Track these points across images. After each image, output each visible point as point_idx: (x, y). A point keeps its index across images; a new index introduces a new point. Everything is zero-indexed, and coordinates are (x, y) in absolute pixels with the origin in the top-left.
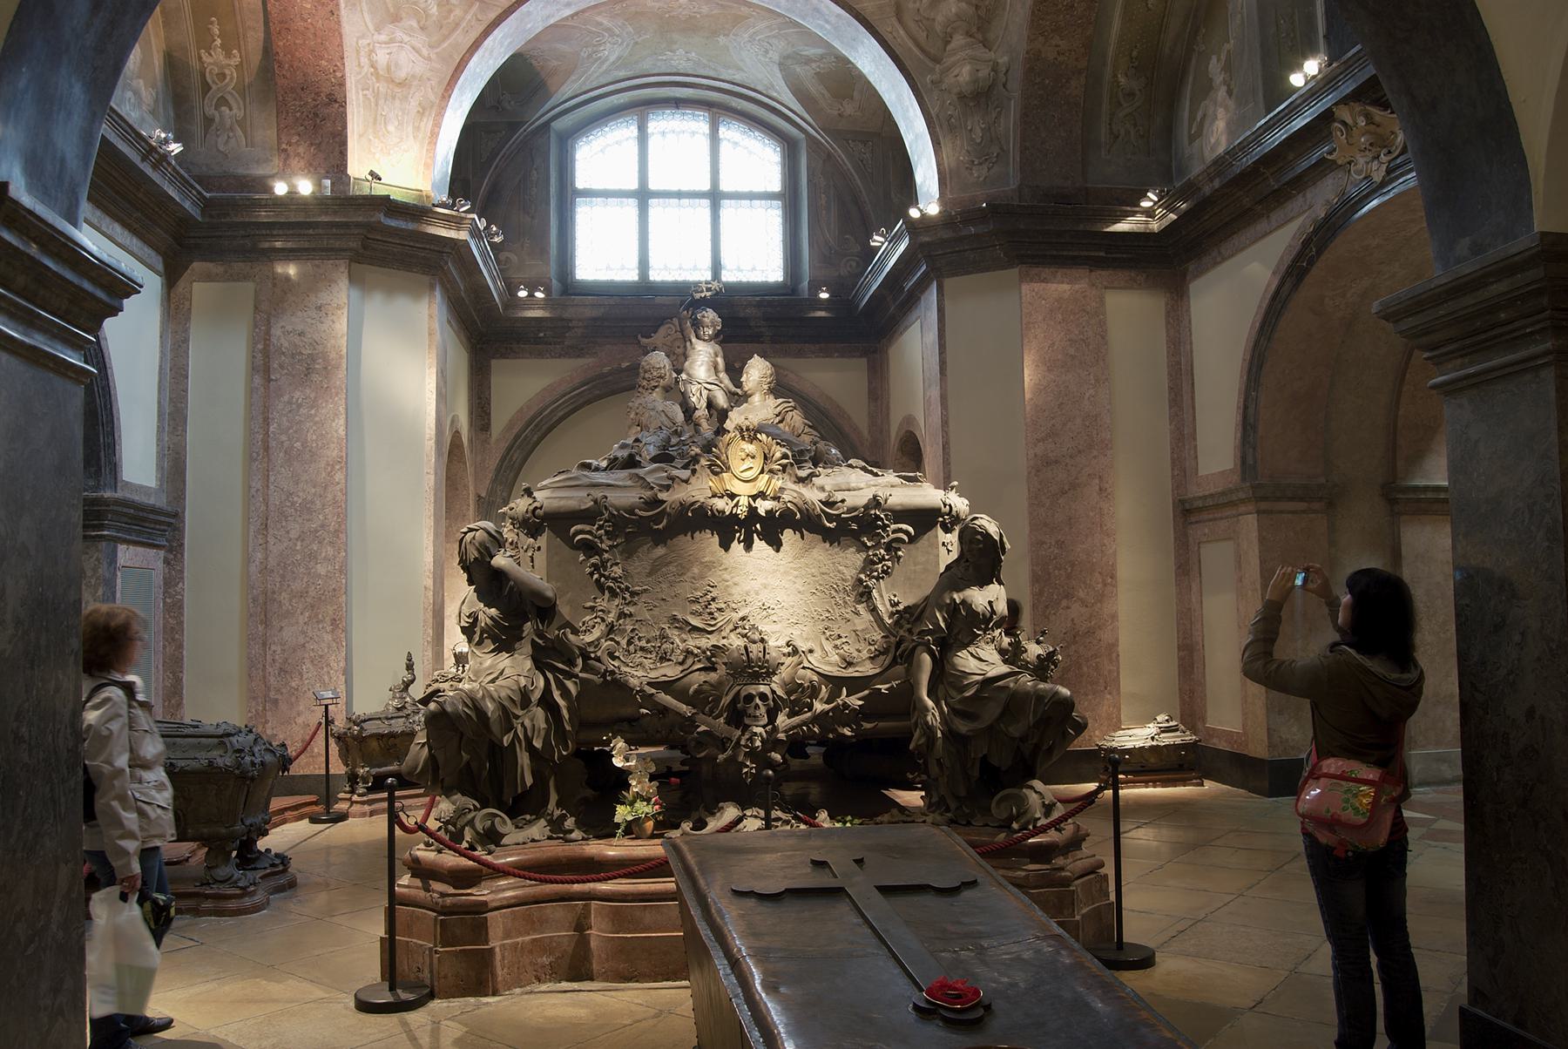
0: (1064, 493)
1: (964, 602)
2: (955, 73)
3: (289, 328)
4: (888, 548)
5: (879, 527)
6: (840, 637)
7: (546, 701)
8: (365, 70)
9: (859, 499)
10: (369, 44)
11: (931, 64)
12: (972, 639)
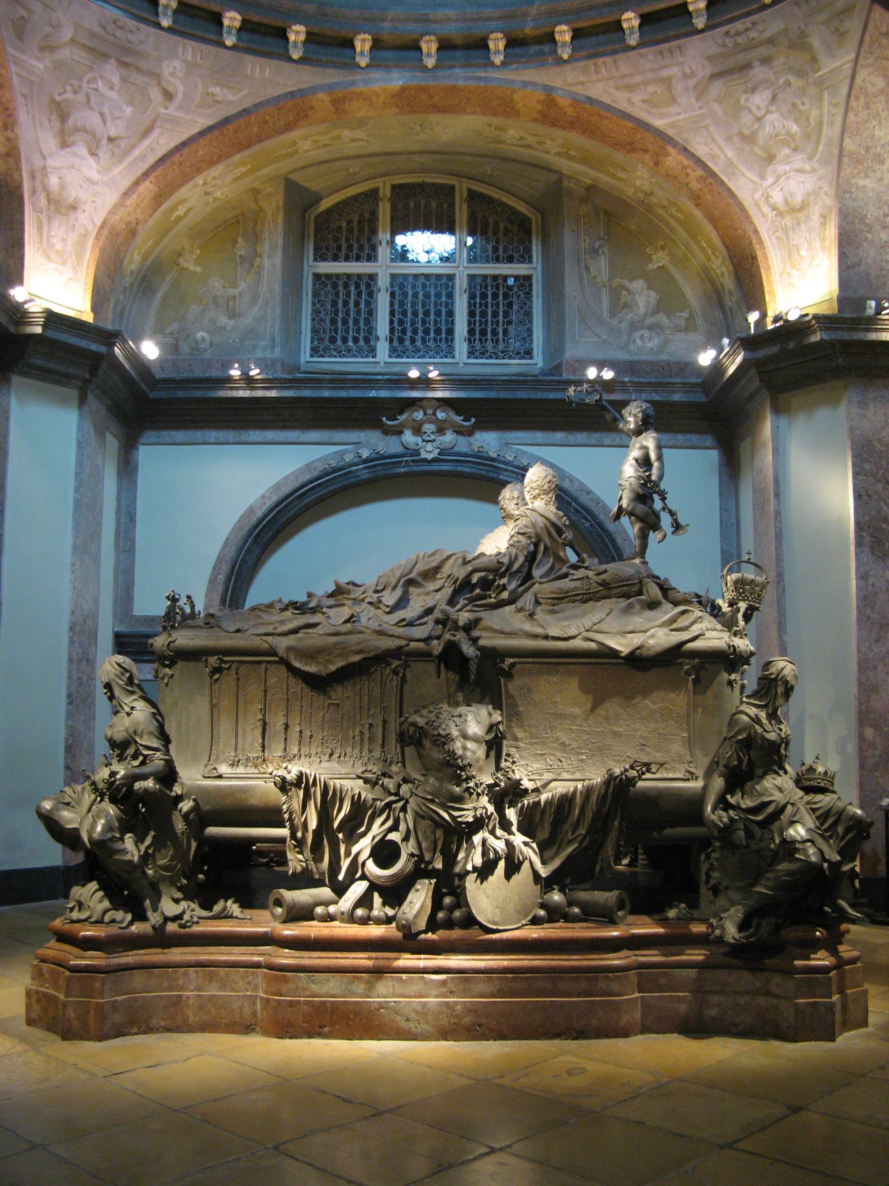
8: (770, 216)
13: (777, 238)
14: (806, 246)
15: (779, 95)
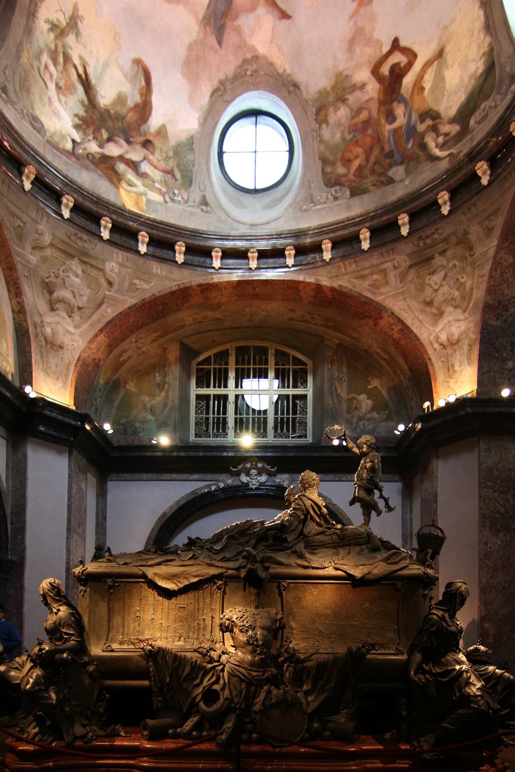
15: (449, 274)
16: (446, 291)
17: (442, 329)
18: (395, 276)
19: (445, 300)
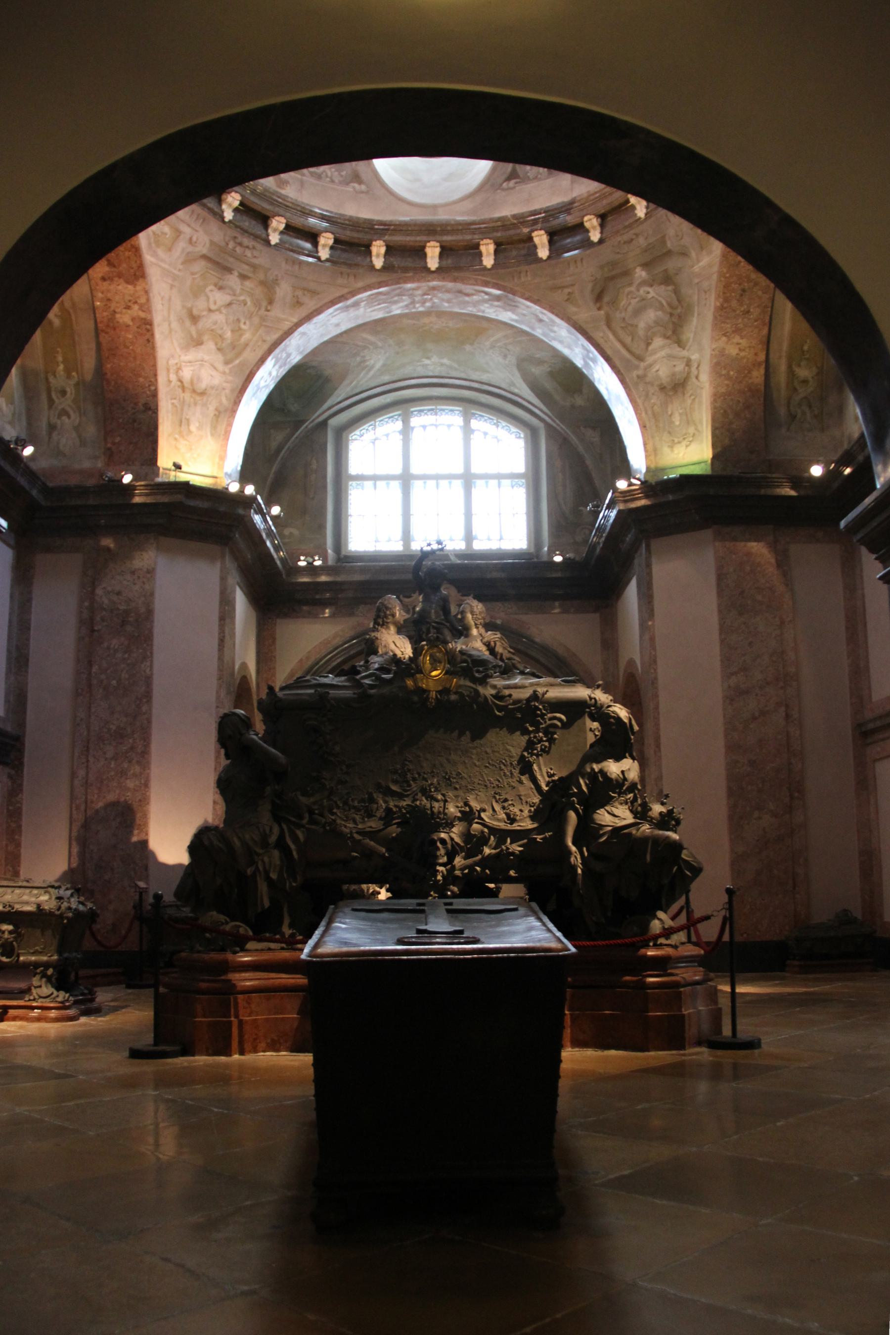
0: (754, 718)
1: (601, 771)
2: (657, 367)
3: (109, 589)
4: (546, 732)
5: (538, 716)
6: (506, 800)
7: (281, 844)
8: (173, 384)
9: (526, 694)
10: (177, 364)
11: (636, 362)
12: (605, 801)
13: (173, 404)
14: (197, 425)
15: (234, 306)
16: (219, 321)
17: (190, 362)
18: (183, 250)
19: (212, 330)
